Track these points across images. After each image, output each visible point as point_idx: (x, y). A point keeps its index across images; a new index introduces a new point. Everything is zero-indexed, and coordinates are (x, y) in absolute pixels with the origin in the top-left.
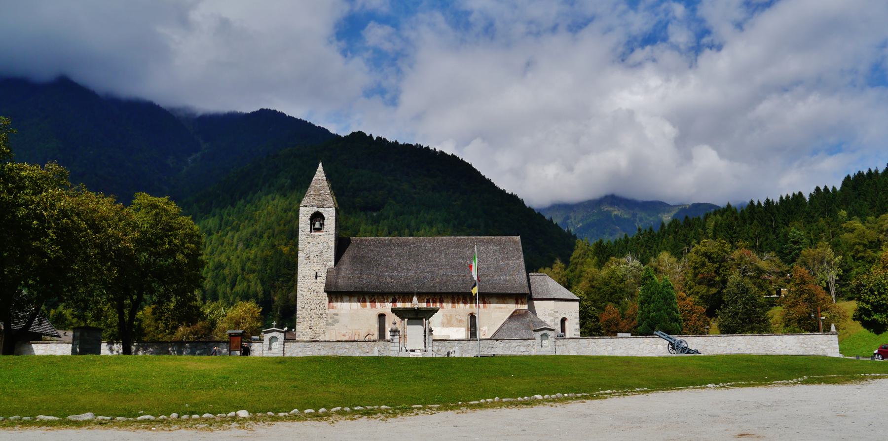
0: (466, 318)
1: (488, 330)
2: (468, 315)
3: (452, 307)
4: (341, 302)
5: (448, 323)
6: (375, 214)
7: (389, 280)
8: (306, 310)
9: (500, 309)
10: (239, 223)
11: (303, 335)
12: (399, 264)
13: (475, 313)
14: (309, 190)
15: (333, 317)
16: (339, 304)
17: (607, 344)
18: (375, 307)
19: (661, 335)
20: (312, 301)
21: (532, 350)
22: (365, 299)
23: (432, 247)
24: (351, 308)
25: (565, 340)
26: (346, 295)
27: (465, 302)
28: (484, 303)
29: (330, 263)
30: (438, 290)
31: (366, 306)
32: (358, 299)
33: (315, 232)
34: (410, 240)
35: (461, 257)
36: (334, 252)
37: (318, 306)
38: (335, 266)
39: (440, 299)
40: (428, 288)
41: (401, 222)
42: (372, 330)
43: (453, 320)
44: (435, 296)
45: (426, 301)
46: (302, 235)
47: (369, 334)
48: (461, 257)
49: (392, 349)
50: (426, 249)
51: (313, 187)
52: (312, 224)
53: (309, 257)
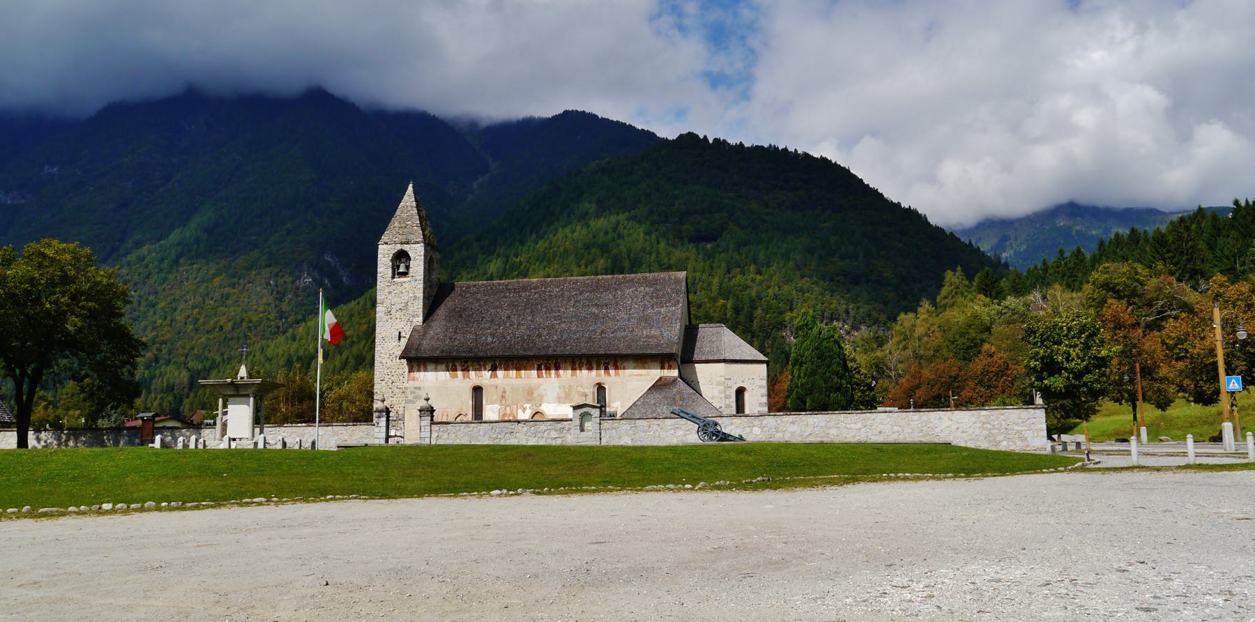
0: (592, 390)
2: (594, 386)
3: (572, 375)
4: (425, 371)
5: (566, 398)
6: (709, 246)
7: (490, 339)
8: (386, 383)
9: (639, 377)
10: (528, 265)
12: (509, 317)
13: (604, 384)
14: (392, 222)
15: (414, 393)
16: (422, 374)
17: (677, 426)
18: (469, 377)
19: (682, 414)
21: (568, 435)
22: (456, 367)
23: (559, 291)
24: (437, 379)
25: (615, 421)
27: (590, 368)
28: (616, 368)
29: (417, 319)
30: (550, 352)
31: (457, 377)
32: (446, 366)
33: (399, 277)
34: (533, 283)
35: (596, 305)
36: (422, 304)
37: (401, 378)
38: (424, 322)
39: (556, 364)
40: (539, 349)
41: (744, 255)
42: (465, 409)
43: (573, 393)
44: (548, 360)
45: (536, 367)
46: (381, 282)
47: (461, 414)
48: (596, 305)
49: (376, 435)
50: (551, 295)
51: (398, 217)
52: (395, 268)
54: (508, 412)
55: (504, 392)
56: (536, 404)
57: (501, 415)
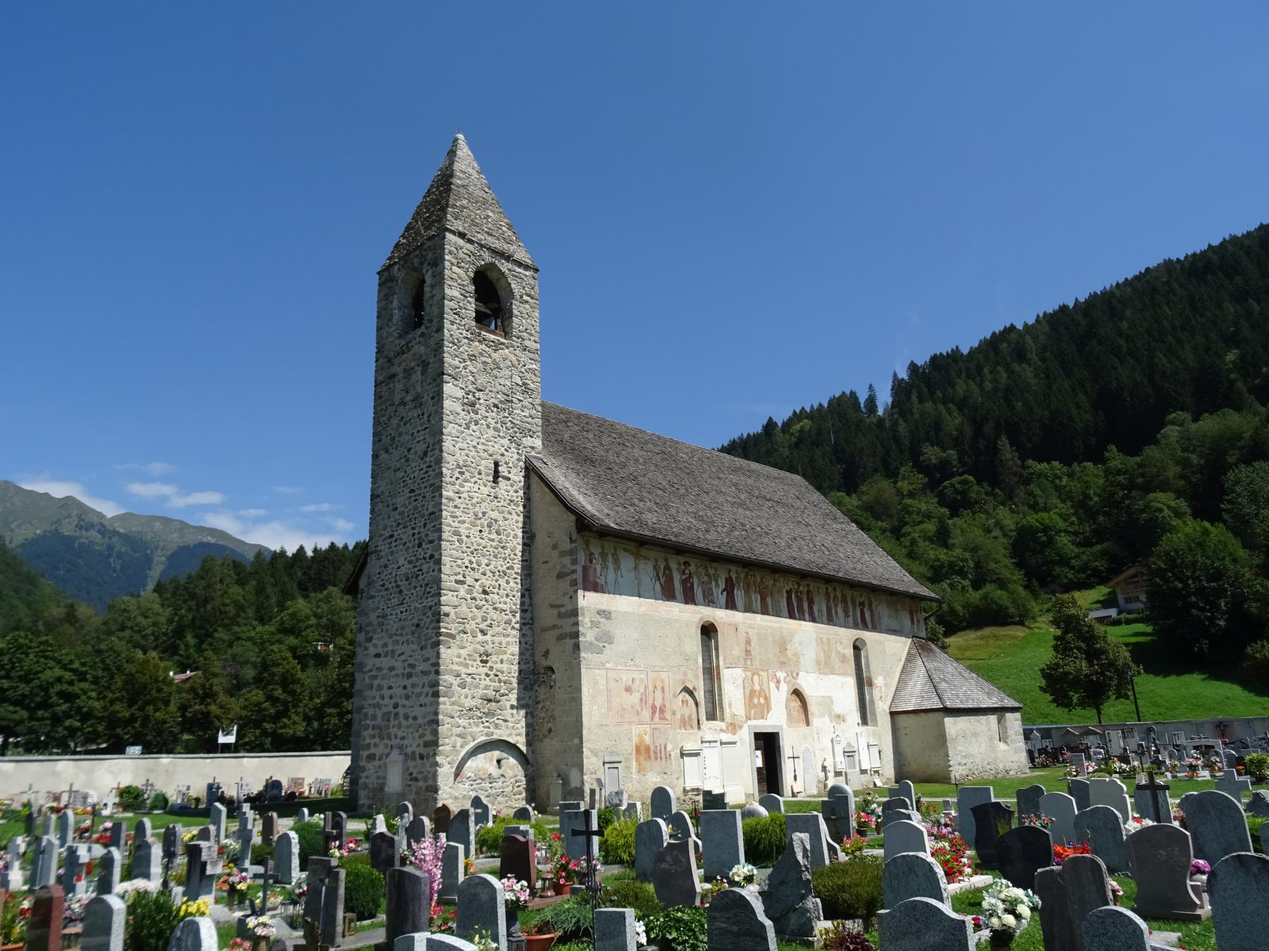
1: (885, 685)
11: (463, 685)
53: (473, 405)
54: (757, 687)
55: (748, 642)
56: (792, 672)
57: (747, 694)
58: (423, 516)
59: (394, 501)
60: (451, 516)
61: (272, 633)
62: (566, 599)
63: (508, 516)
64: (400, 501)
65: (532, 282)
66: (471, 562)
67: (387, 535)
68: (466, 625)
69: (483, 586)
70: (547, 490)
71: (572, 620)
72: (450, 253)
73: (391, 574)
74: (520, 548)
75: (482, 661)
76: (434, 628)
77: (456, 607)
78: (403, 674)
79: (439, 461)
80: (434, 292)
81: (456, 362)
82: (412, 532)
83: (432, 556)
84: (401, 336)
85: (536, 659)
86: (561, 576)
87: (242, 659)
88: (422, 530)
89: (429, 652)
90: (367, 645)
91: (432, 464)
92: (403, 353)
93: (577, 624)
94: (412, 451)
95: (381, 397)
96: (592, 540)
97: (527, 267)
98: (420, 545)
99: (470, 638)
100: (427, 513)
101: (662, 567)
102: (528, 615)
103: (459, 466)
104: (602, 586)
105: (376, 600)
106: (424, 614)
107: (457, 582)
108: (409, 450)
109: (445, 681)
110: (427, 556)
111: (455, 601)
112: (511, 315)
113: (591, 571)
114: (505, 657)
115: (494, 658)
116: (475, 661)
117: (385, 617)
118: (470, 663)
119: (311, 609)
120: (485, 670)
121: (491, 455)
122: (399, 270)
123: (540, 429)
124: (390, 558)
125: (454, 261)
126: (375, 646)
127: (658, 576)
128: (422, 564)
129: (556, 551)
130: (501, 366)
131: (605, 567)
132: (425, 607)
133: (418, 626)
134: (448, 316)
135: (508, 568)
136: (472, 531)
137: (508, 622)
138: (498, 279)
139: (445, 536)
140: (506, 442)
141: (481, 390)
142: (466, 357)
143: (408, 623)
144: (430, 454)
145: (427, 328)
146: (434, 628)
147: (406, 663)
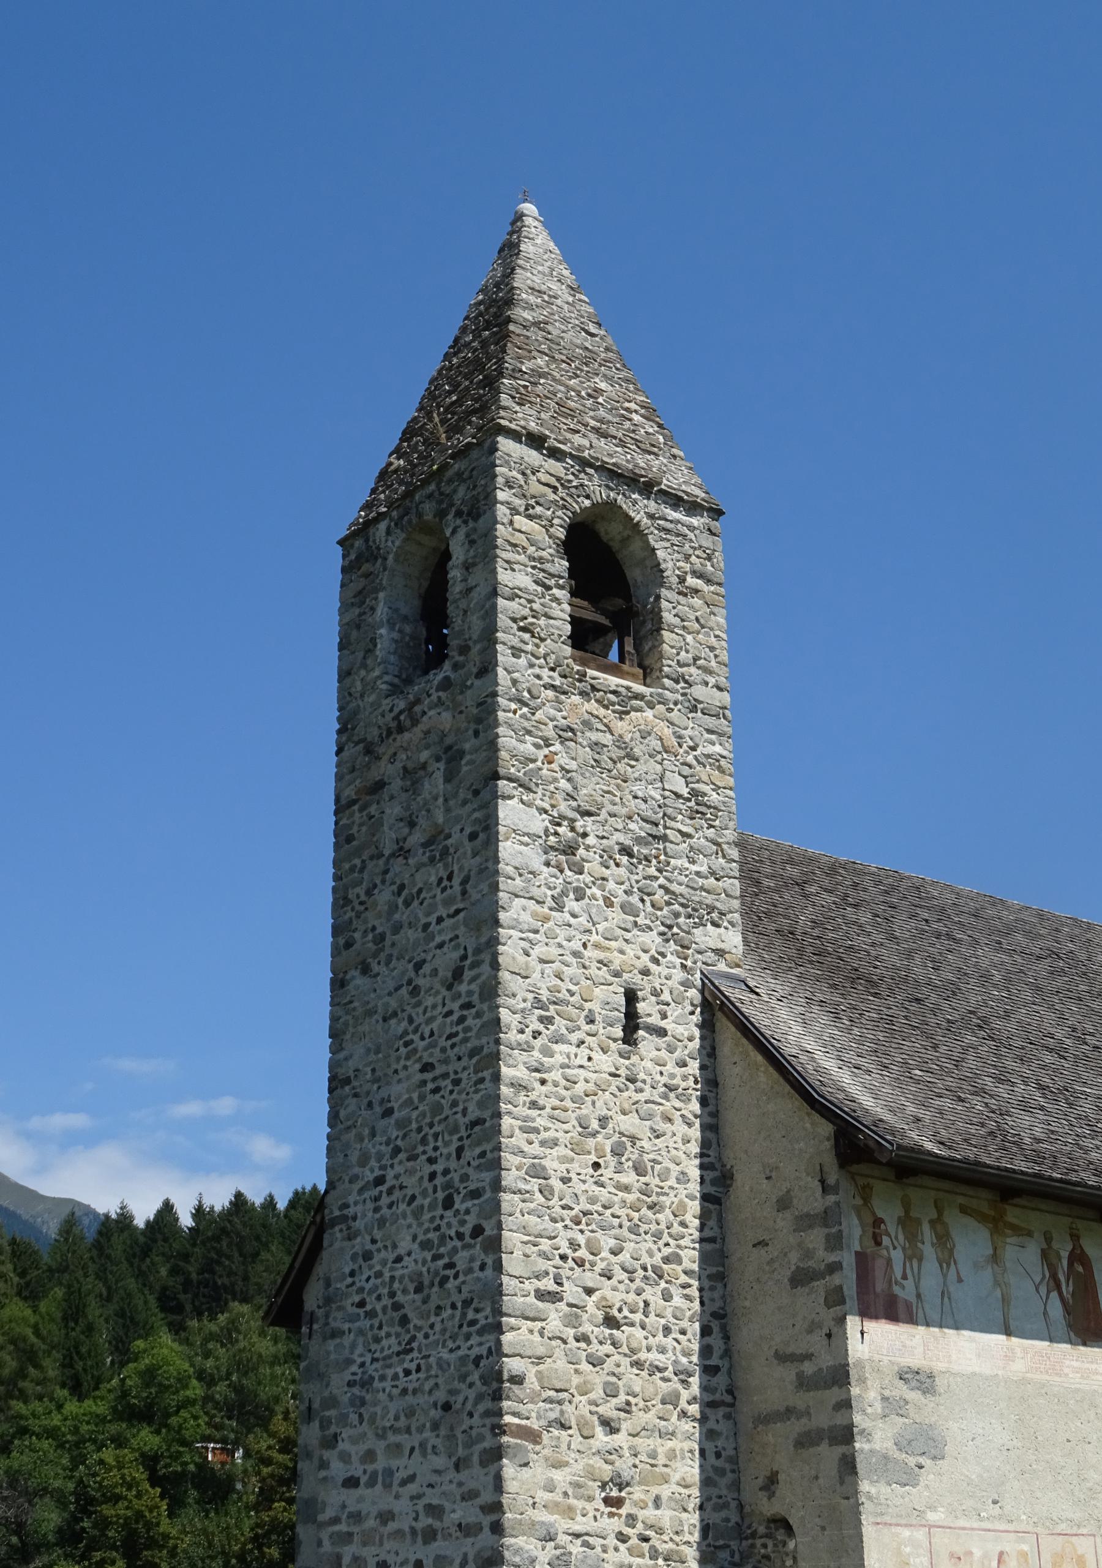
8: (573, 1321)
20: (607, 1242)
26: (964, 1210)
32: (1045, 1255)
37: (653, 1294)
53: (570, 850)
58: (455, 1130)
59: (383, 1093)
60: (525, 1130)
61: (101, 1420)
62: (818, 1338)
63: (662, 1126)
64: (398, 1091)
65: (707, 541)
66: (574, 1245)
67: (370, 1177)
68: (568, 1408)
69: (605, 1306)
70: (760, 1058)
71: (833, 1395)
72: (509, 484)
73: (379, 1274)
74: (694, 1207)
75: (607, 1501)
76: (487, 1414)
77: (540, 1359)
78: (413, 1532)
79: (491, 991)
80: (471, 582)
81: (527, 747)
82: (428, 1169)
83: (478, 1231)
84: (395, 690)
85: (746, 1496)
86: (801, 1278)
87: (32, 1483)
88: (453, 1164)
89: (476, 1477)
90: (327, 1454)
91: (475, 998)
92: (401, 729)
93: (846, 1404)
94: (427, 969)
95: (349, 839)
96: (878, 1186)
97: (693, 507)
98: (448, 1203)
99: (577, 1441)
100: (462, 1121)
101: (1065, 1255)
102: (721, 1380)
103: (539, 1004)
104: (908, 1305)
105: (347, 1340)
106: (463, 1378)
107: (541, 1295)
108: (418, 966)
109: (517, 1551)
110: (467, 1229)
111: (538, 1345)
112: (658, 625)
113: (880, 1264)
114: (665, 1491)
115: (637, 1493)
116: (590, 1499)
117: (366, 1383)
118: (579, 1504)
119: (190, 1359)
120: (616, 1524)
121: (617, 975)
122: (388, 532)
123: (736, 904)
124: (378, 1234)
125: (519, 503)
126: (345, 1458)
127: (1054, 1277)
128: (455, 1250)
129: (788, 1214)
130: (637, 751)
131: (914, 1255)
132: (463, 1359)
133: (447, 1407)
134: (507, 636)
135: (667, 1260)
136: (575, 1167)
137: (671, 1400)
138: (626, 540)
139: (509, 1178)
140: (652, 940)
141: (589, 814)
142: (550, 732)
143: (422, 1399)
144: (468, 974)
145: (456, 667)
146: (487, 1414)
147: (421, 1503)
